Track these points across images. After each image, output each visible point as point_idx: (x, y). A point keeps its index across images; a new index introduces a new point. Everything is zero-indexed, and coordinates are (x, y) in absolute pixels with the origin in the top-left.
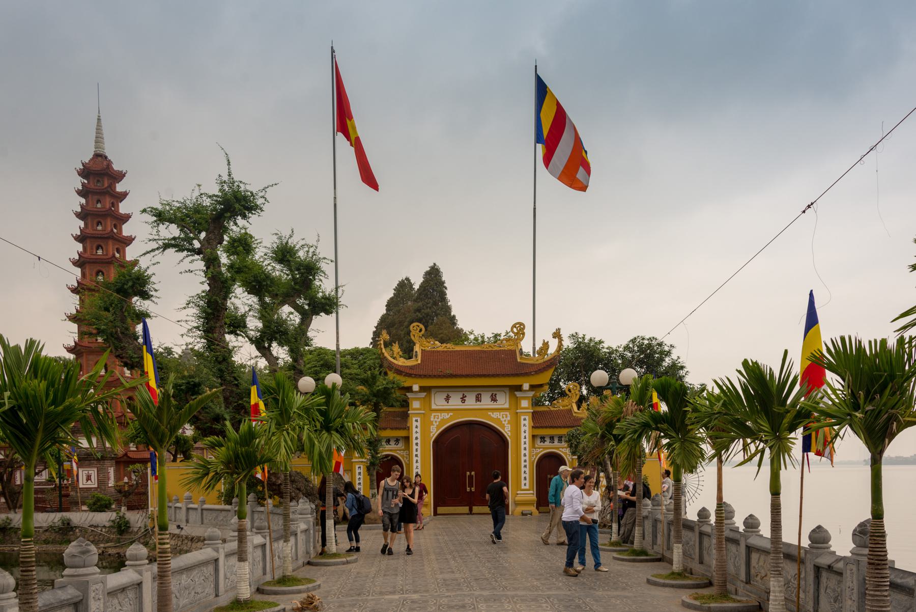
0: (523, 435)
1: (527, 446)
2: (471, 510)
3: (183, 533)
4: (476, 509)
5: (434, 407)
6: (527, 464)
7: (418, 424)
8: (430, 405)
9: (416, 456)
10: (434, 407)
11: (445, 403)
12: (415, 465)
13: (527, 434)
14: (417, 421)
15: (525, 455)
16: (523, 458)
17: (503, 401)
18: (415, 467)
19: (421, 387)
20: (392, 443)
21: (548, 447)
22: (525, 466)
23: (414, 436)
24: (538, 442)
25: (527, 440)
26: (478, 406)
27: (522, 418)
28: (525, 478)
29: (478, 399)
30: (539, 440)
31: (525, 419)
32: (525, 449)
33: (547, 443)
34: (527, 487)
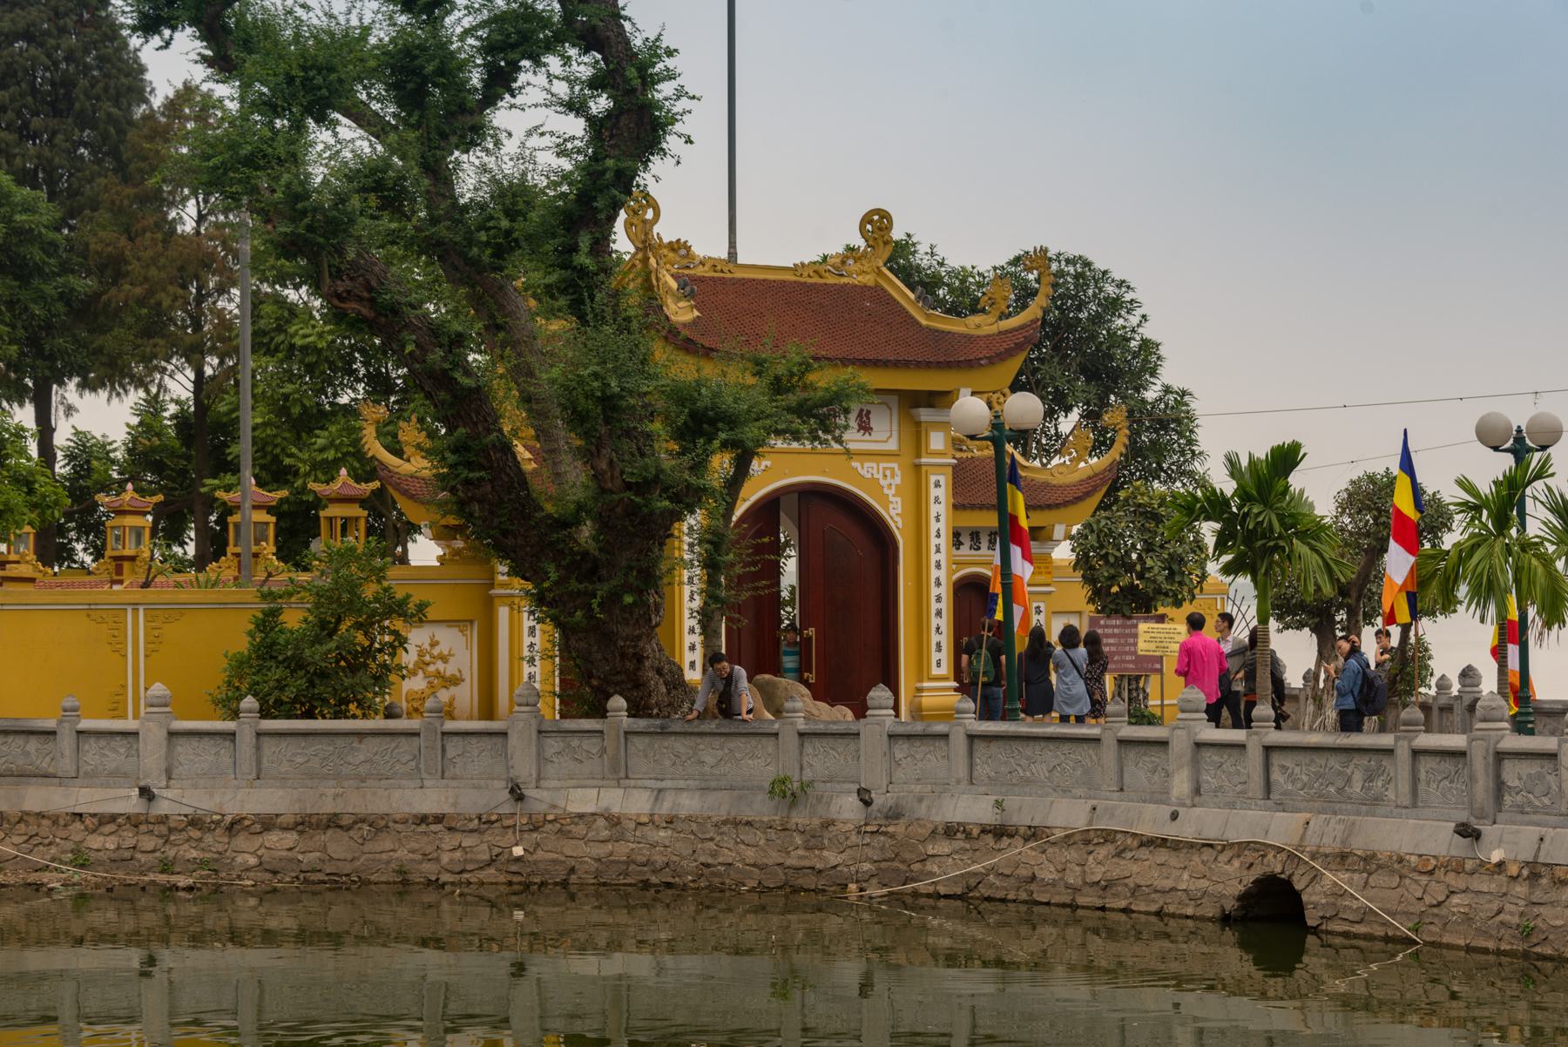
0: (934, 526)
3: (162, 808)
13: (942, 525)
22: (939, 613)
27: (933, 479)
31: (937, 485)
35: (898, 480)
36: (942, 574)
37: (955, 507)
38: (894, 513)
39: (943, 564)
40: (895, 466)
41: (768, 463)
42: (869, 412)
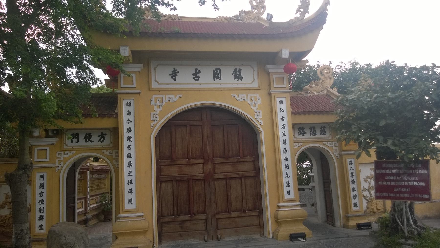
8: (149, 83)
9: (129, 156)
10: (154, 85)
12: (126, 170)
14: (129, 104)
16: (283, 156)
17: (250, 78)
18: (126, 173)
19: (133, 52)
20: (95, 138)
21: (310, 141)
22: (287, 167)
23: (125, 126)
25: (286, 130)
26: (217, 84)
27: (278, 100)
29: (217, 76)
31: (281, 102)
32: (285, 142)
33: (307, 136)
35: (259, 102)
36: (288, 147)
37: (292, 113)
39: (288, 141)
42: (240, 70)
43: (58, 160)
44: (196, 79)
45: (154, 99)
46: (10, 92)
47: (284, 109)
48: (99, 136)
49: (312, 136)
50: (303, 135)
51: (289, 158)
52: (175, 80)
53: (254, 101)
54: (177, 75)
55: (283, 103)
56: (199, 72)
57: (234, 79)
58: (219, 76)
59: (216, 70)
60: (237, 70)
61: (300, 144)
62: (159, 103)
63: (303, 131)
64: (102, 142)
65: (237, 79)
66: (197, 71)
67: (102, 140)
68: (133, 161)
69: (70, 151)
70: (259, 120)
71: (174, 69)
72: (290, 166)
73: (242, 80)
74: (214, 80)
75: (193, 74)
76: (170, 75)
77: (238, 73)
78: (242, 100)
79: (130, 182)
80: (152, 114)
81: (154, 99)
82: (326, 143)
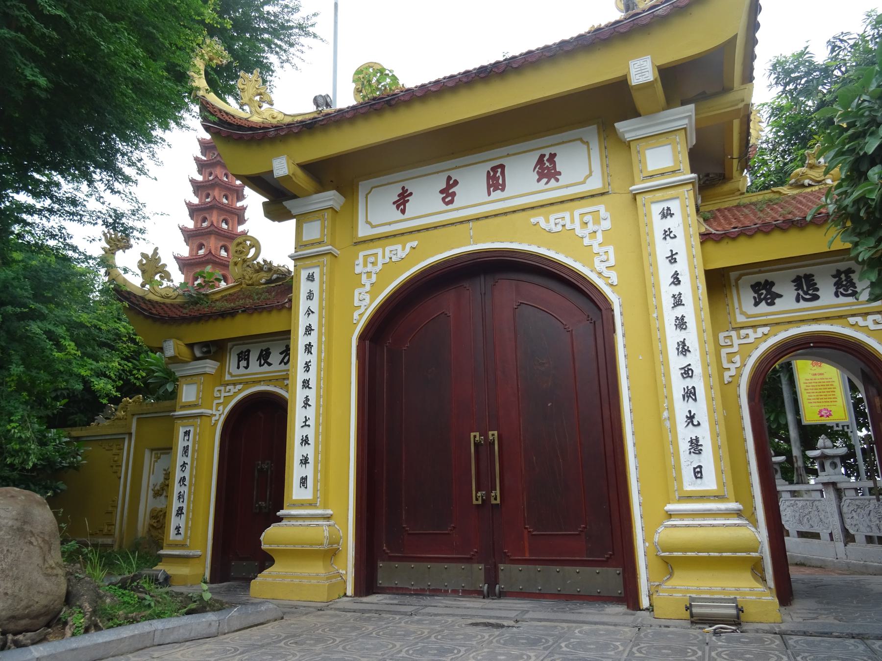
0: (665, 272)
1: (688, 311)
2: (492, 578)
4: (511, 573)
5: (363, 231)
6: (698, 383)
7: (315, 287)
8: (354, 227)
9: (306, 384)
11: (398, 215)
13: (682, 266)
14: (311, 278)
15: (683, 349)
16: (676, 362)
17: (581, 167)
22: (690, 394)
24: (745, 306)
26: (499, 201)
28: (695, 446)
30: (748, 297)
31: (667, 214)
32: (681, 324)
33: (788, 303)
34: (709, 483)
37: (705, 238)
38: (601, 269)
40: (602, 208)
41: (415, 244)
42: (553, 156)
43: (216, 402)
44: (450, 198)
45: (361, 260)
46: (143, 285)
47: (678, 231)
48: (281, 353)
49: (803, 304)
50: (772, 304)
51: (697, 369)
52: (403, 212)
53: (590, 225)
54: (408, 201)
55: (672, 215)
56: (456, 183)
57: (539, 180)
58: (500, 181)
59: (494, 169)
60: (545, 159)
61: (761, 331)
62: (370, 268)
63: (769, 292)
64: (286, 364)
65: (545, 180)
66: (451, 182)
67: (285, 360)
68: (312, 394)
69: (234, 384)
70: (606, 273)
71: (403, 188)
72: (701, 393)
73: (557, 180)
74: (489, 194)
75: (442, 192)
76: (394, 203)
77: (547, 164)
78: (559, 228)
79: (305, 441)
80: (356, 292)
81: (361, 260)
82: (859, 320)
